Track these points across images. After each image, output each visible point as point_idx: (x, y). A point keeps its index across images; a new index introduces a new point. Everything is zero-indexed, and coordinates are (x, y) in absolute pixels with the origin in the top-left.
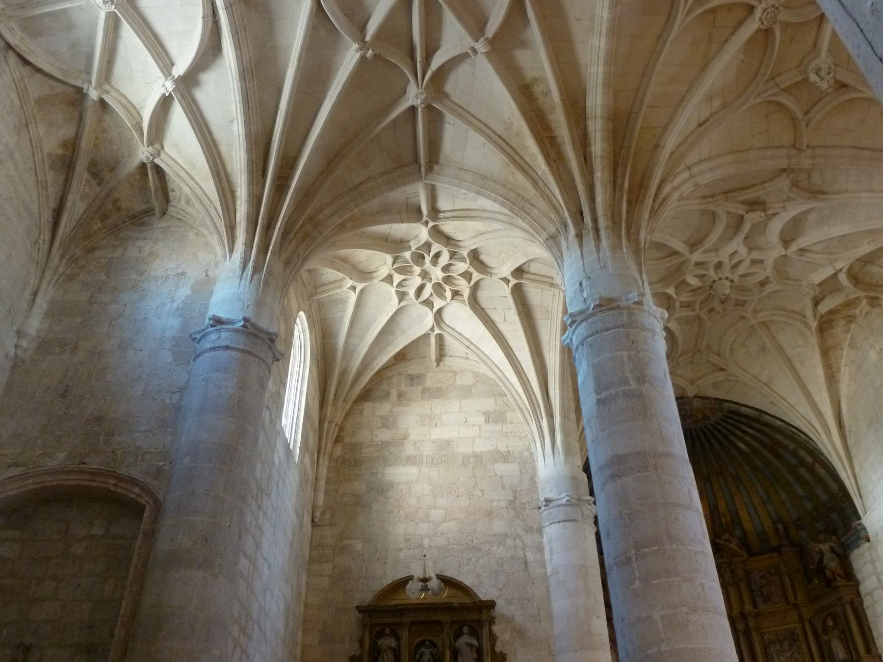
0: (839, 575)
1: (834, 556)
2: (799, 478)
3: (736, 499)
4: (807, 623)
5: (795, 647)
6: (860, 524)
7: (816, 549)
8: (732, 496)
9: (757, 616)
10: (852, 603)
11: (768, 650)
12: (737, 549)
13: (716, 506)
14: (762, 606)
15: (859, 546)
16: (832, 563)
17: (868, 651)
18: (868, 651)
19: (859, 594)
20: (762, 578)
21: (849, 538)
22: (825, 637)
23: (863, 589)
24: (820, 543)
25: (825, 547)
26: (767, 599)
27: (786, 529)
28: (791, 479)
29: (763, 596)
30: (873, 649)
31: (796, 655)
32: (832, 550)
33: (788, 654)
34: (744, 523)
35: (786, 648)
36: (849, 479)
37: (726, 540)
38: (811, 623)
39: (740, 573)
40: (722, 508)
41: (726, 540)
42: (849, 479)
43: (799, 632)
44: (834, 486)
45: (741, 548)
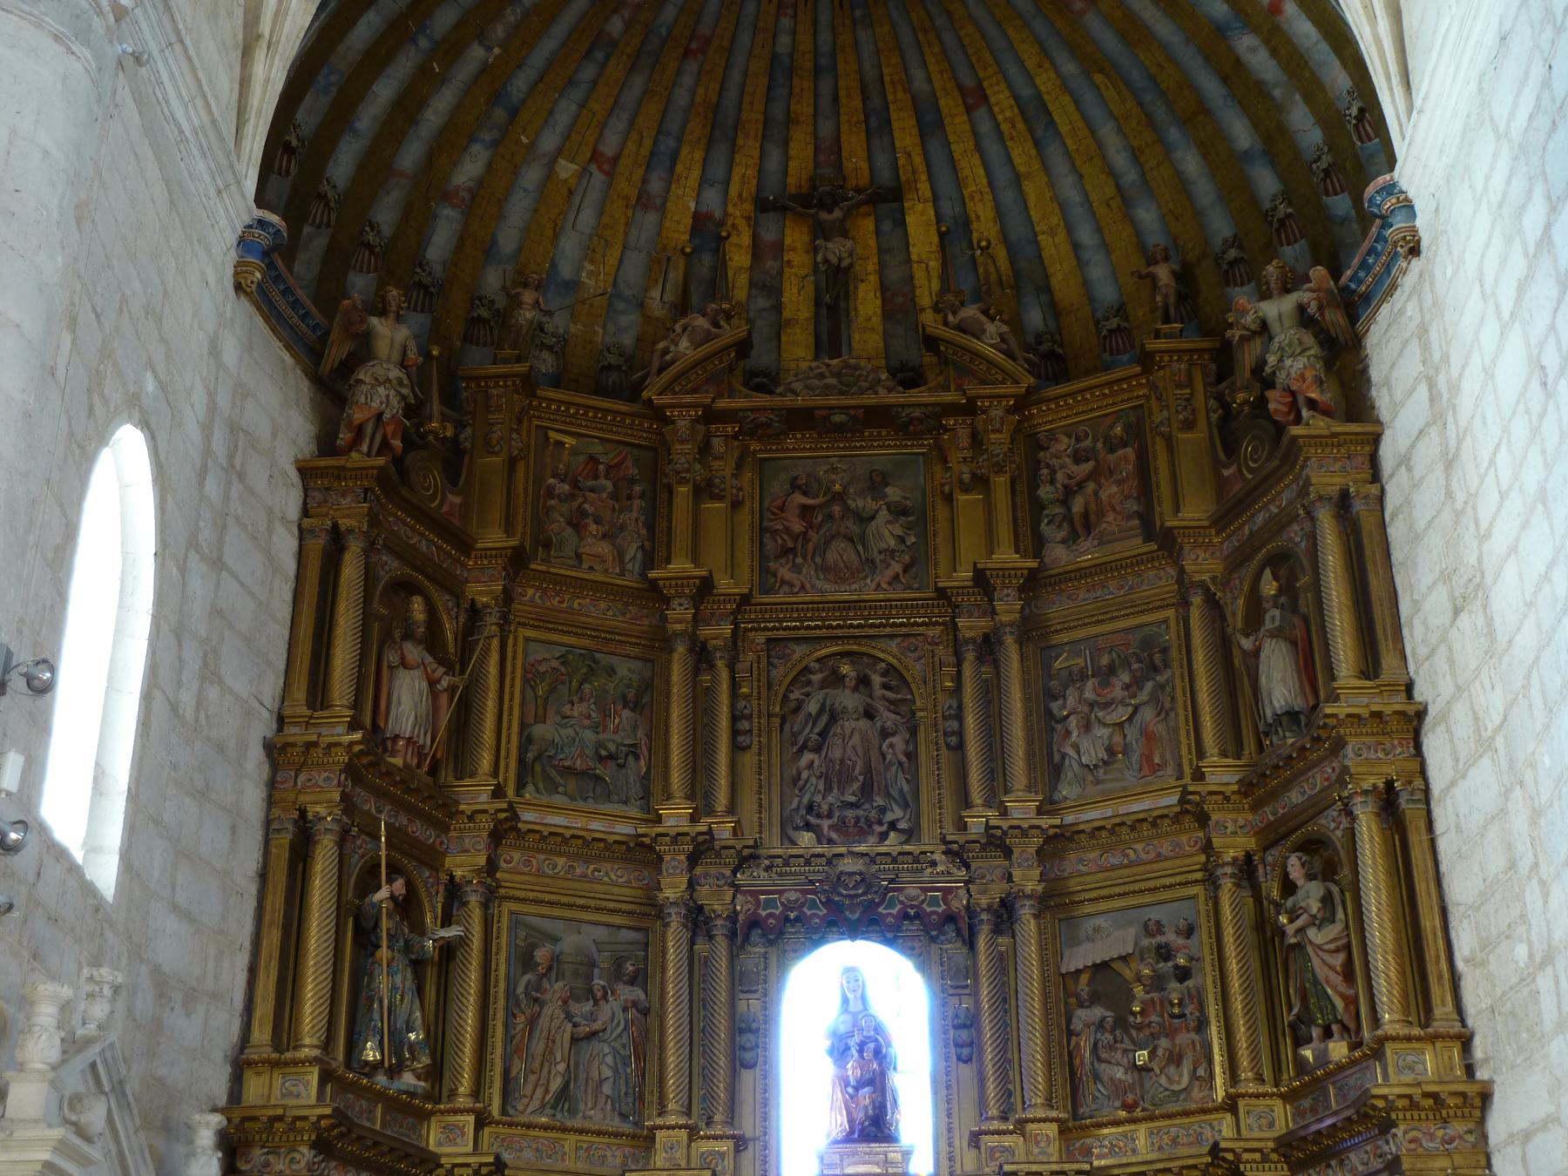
0: (1312, 404)
1: (1309, 339)
2: (1233, 74)
3: (1028, 187)
4: (1197, 600)
5: (1149, 686)
6: (1391, 189)
7: (1249, 320)
8: (1018, 178)
9: (1033, 583)
10: (1343, 502)
11: (1055, 706)
12: (1000, 358)
13: (965, 224)
14: (1058, 555)
15: (1394, 287)
16: (1296, 364)
17: (1370, 665)
18: (1370, 665)
19: (1376, 477)
20: (1077, 460)
21: (1364, 265)
22: (1247, 644)
23: (1388, 453)
24: (1265, 296)
25: (1277, 309)
26: (1082, 527)
27: (1184, 276)
28: (1211, 87)
29: (1068, 518)
30: (1388, 661)
31: (1148, 714)
32: (1304, 318)
33: (1121, 714)
34: (1056, 281)
35: (1118, 693)
36: (1372, 18)
37: (961, 328)
38: (1212, 603)
39: (999, 441)
40: (985, 227)
41: (961, 328)
42: (1372, 18)
43: (1171, 636)
44: (1339, 79)
45: (1009, 354)
